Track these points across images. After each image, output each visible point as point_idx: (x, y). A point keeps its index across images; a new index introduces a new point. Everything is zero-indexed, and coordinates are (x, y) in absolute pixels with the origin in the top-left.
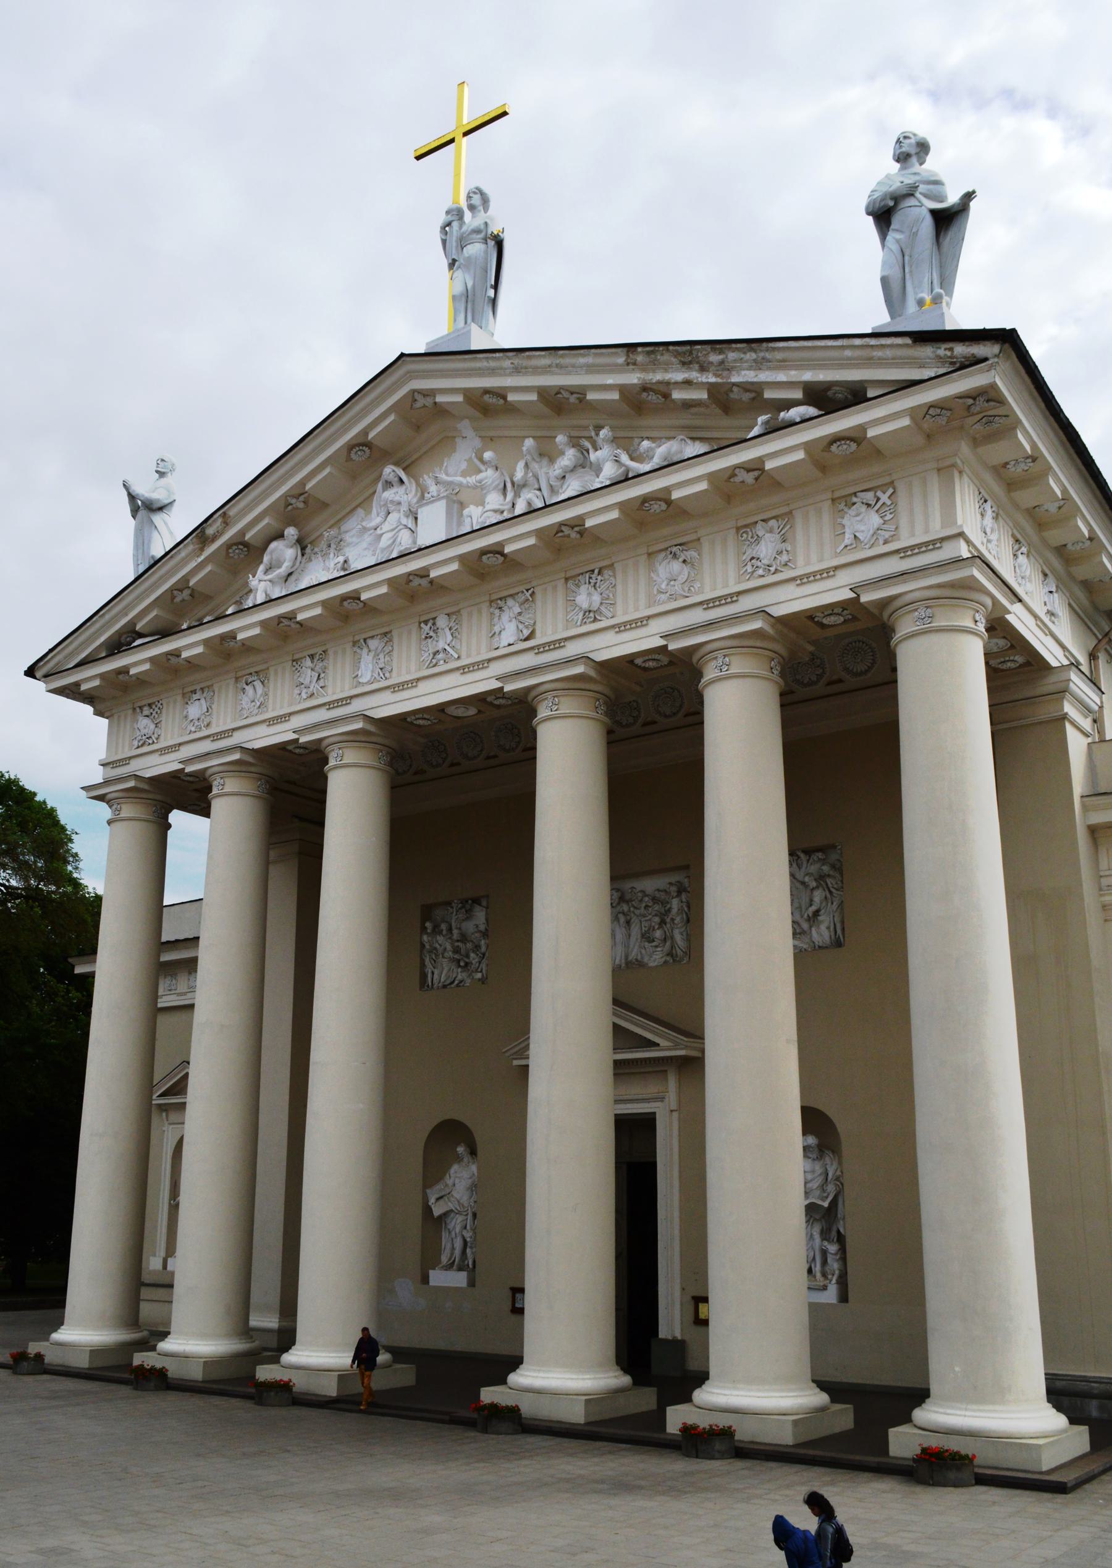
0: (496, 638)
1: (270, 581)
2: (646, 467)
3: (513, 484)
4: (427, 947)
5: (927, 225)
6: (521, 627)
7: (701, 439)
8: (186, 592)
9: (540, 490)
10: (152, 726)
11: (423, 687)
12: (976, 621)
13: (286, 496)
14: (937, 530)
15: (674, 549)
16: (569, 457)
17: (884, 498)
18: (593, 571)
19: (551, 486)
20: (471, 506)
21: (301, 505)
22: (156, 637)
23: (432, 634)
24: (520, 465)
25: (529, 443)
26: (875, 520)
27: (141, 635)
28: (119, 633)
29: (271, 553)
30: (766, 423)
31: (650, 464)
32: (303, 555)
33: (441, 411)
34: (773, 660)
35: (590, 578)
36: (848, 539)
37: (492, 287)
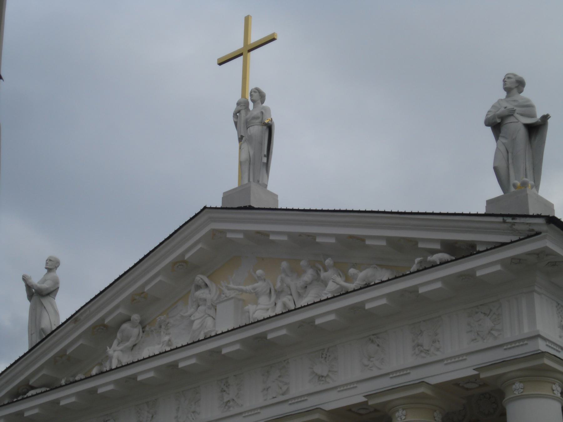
1: (121, 351)
3: (275, 291)
7: (387, 267)
9: (291, 295)
12: (553, 390)
14: (527, 331)
16: (308, 276)
19: (299, 293)
20: (249, 305)
22: (43, 389)
24: (279, 280)
25: (284, 264)
27: (33, 388)
28: (18, 386)
30: (420, 262)
31: (355, 284)
32: (143, 332)
34: (435, 411)
35: (322, 354)
37: (265, 156)
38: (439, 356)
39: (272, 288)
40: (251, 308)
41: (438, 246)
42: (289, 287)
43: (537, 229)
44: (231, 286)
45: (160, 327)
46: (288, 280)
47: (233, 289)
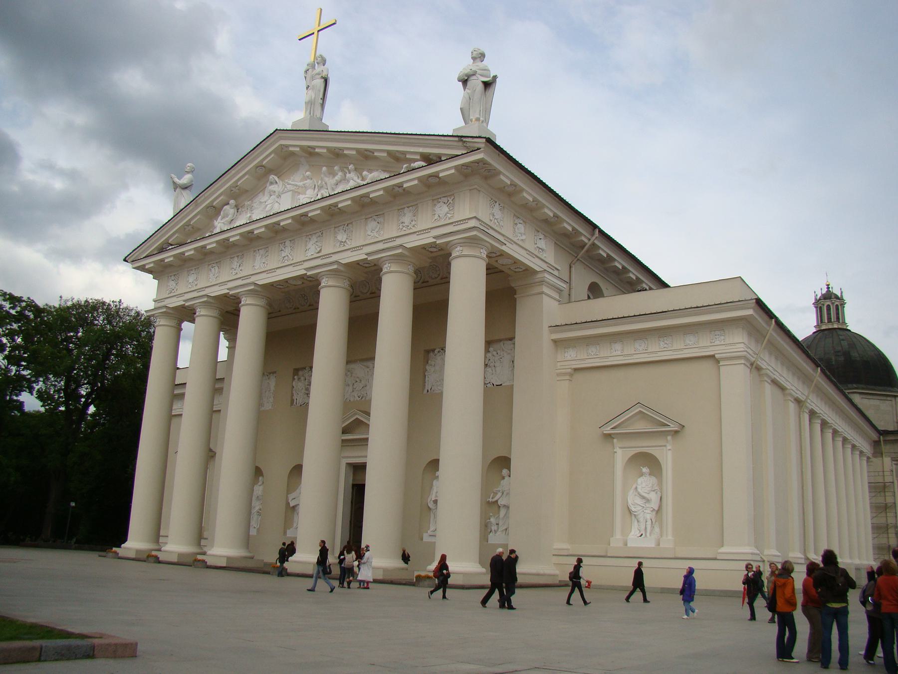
0: (307, 252)
1: (223, 223)
2: (365, 183)
4: (295, 387)
5: (481, 86)
6: (317, 247)
8: (190, 227)
10: (175, 285)
11: (279, 271)
13: (230, 187)
15: (375, 217)
17: (450, 201)
18: (345, 225)
21: (237, 191)
23: (284, 249)
25: (324, 169)
26: (445, 209)
28: (163, 243)
29: (225, 210)
30: (407, 167)
33: (293, 154)
36: (436, 216)
38: (414, 230)
39: (316, 184)
40: (301, 197)
41: (418, 157)
42: (326, 183)
43: (477, 146)
44: (290, 182)
45: (248, 209)
46: (326, 179)
47: (291, 184)
